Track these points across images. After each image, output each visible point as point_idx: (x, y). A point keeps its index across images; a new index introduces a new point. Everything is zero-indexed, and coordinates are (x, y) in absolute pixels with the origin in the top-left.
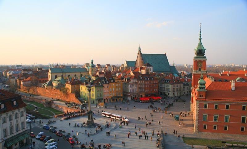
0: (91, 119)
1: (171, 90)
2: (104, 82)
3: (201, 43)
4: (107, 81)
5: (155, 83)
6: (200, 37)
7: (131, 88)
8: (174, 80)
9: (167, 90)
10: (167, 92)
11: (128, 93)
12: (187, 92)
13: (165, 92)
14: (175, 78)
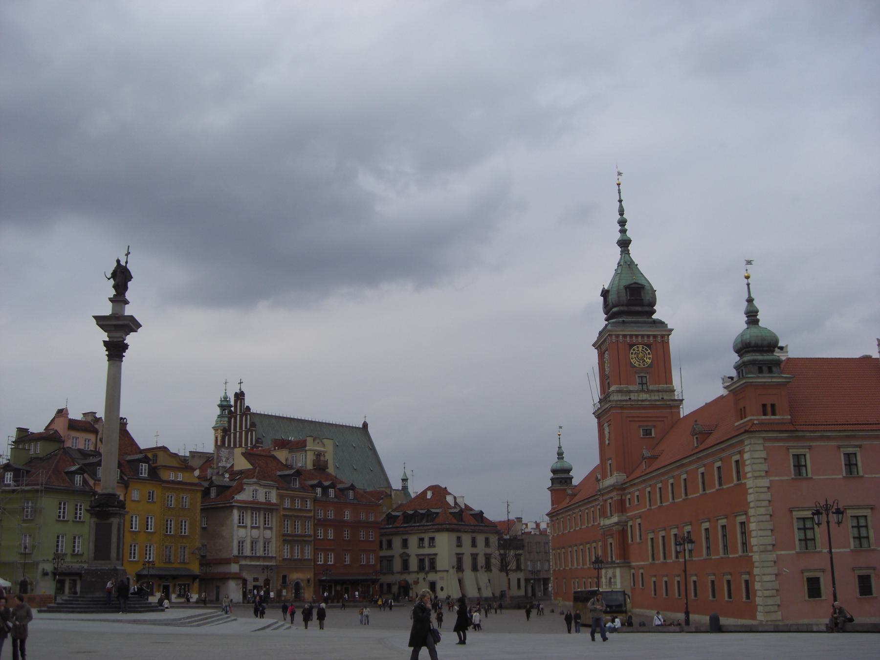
1: (441, 564)
3: (632, 262)
5: (363, 517)
6: (623, 231)
7: (242, 533)
9: (421, 562)
10: (421, 576)
11: (228, 562)
12: (519, 580)
13: (411, 578)
14: (456, 503)
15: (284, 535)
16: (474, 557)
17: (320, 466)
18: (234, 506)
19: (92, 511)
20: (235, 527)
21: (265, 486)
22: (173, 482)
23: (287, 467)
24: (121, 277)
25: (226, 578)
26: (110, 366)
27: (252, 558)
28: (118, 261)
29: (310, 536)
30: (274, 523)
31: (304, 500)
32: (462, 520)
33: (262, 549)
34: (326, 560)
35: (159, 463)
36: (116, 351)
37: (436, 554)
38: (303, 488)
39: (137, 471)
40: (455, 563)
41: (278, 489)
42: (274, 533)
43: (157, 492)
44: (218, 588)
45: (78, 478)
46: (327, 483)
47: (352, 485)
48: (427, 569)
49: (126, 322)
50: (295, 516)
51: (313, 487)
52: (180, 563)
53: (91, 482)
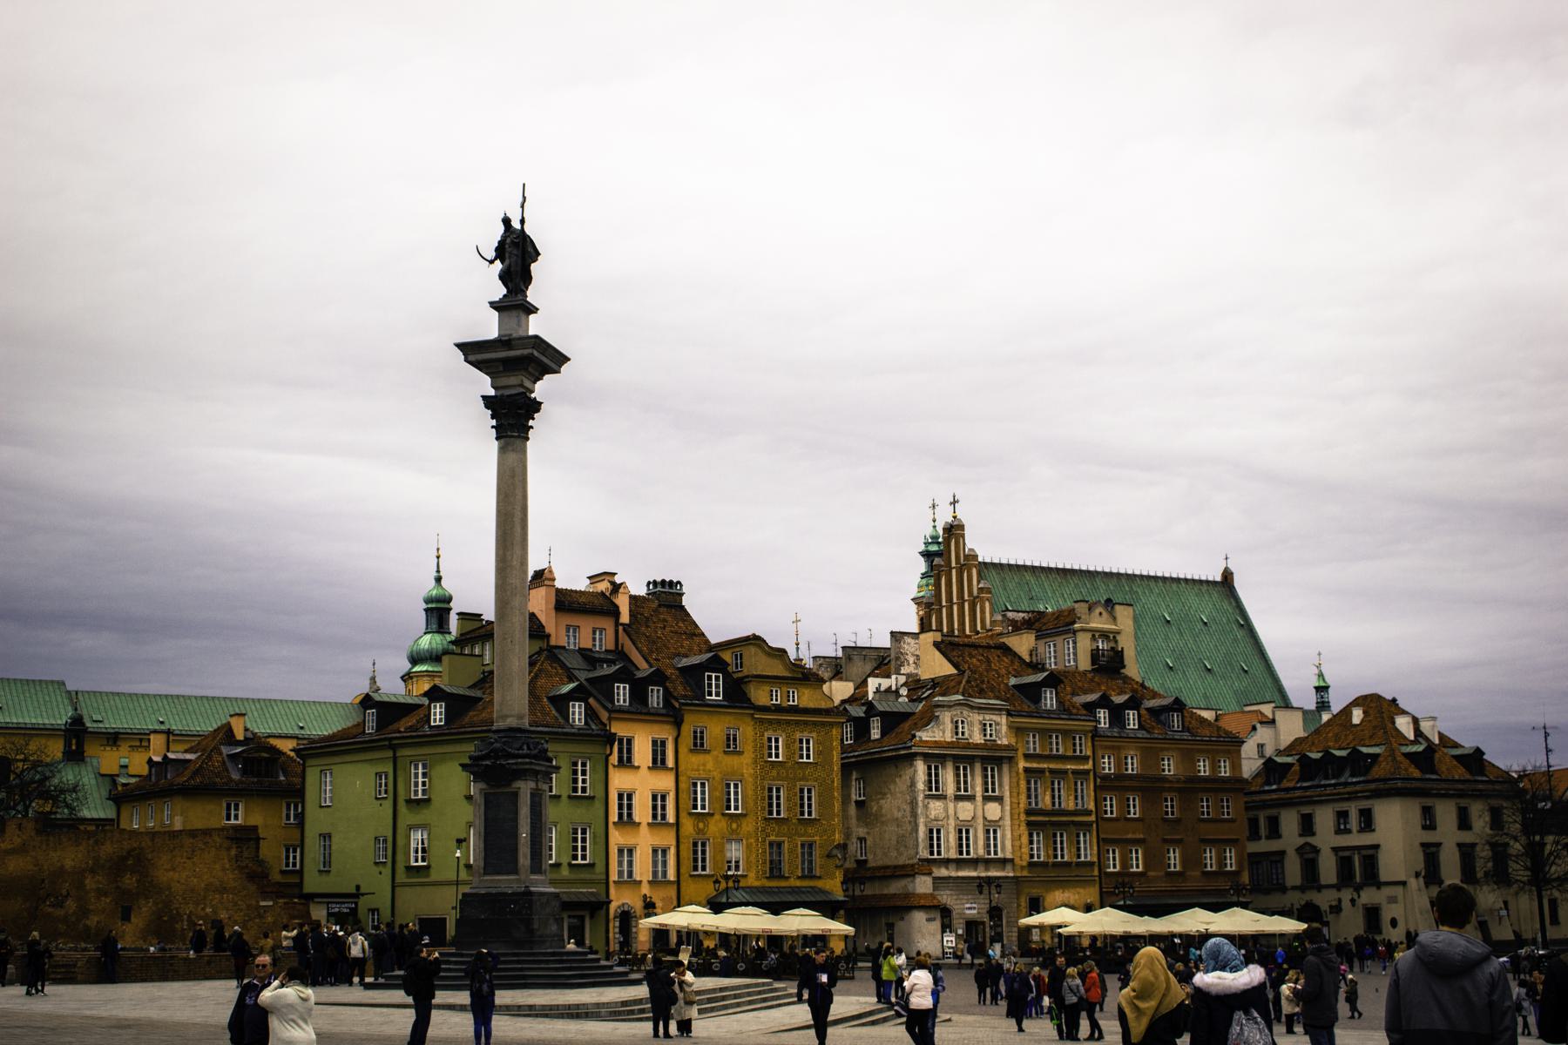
0: (524, 858)
2: (622, 693)
4: (658, 678)
5: (1204, 769)
7: (936, 807)
8: (1420, 748)
9: (1344, 865)
10: (1346, 895)
11: (908, 871)
13: (1324, 900)
14: (1418, 733)
15: (1029, 812)
16: (1467, 851)
17: (1109, 664)
18: (915, 755)
19: (475, 768)
20: (921, 797)
21: (980, 709)
22: (778, 709)
23: (1036, 666)
24: (516, 254)
25: (904, 906)
26: (502, 450)
27: (960, 863)
28: (507, 222)
29: (1089, 813)
30: (1007, 788)
31: (1067, 734)
32: (1434, 772)
33: (981, 842)
34: (1125, 863)
35: (746, 672)
36: (512, 417)
37: (1377, 847)
38: (1064, 709)
39: (699, 691)
40: (1421, 866)
41: (1009, 714)
42: (1008, 808)
43: (746, 731)
44: (891, 926)
45: (577, 712)
46: (1119, 699)
47: (1177, 701)
48: (1358, 879)
49: (526, 352)
50: (1052, 771)
51: (1090, 708)
52: (803, 877)
53: (604, 715)
